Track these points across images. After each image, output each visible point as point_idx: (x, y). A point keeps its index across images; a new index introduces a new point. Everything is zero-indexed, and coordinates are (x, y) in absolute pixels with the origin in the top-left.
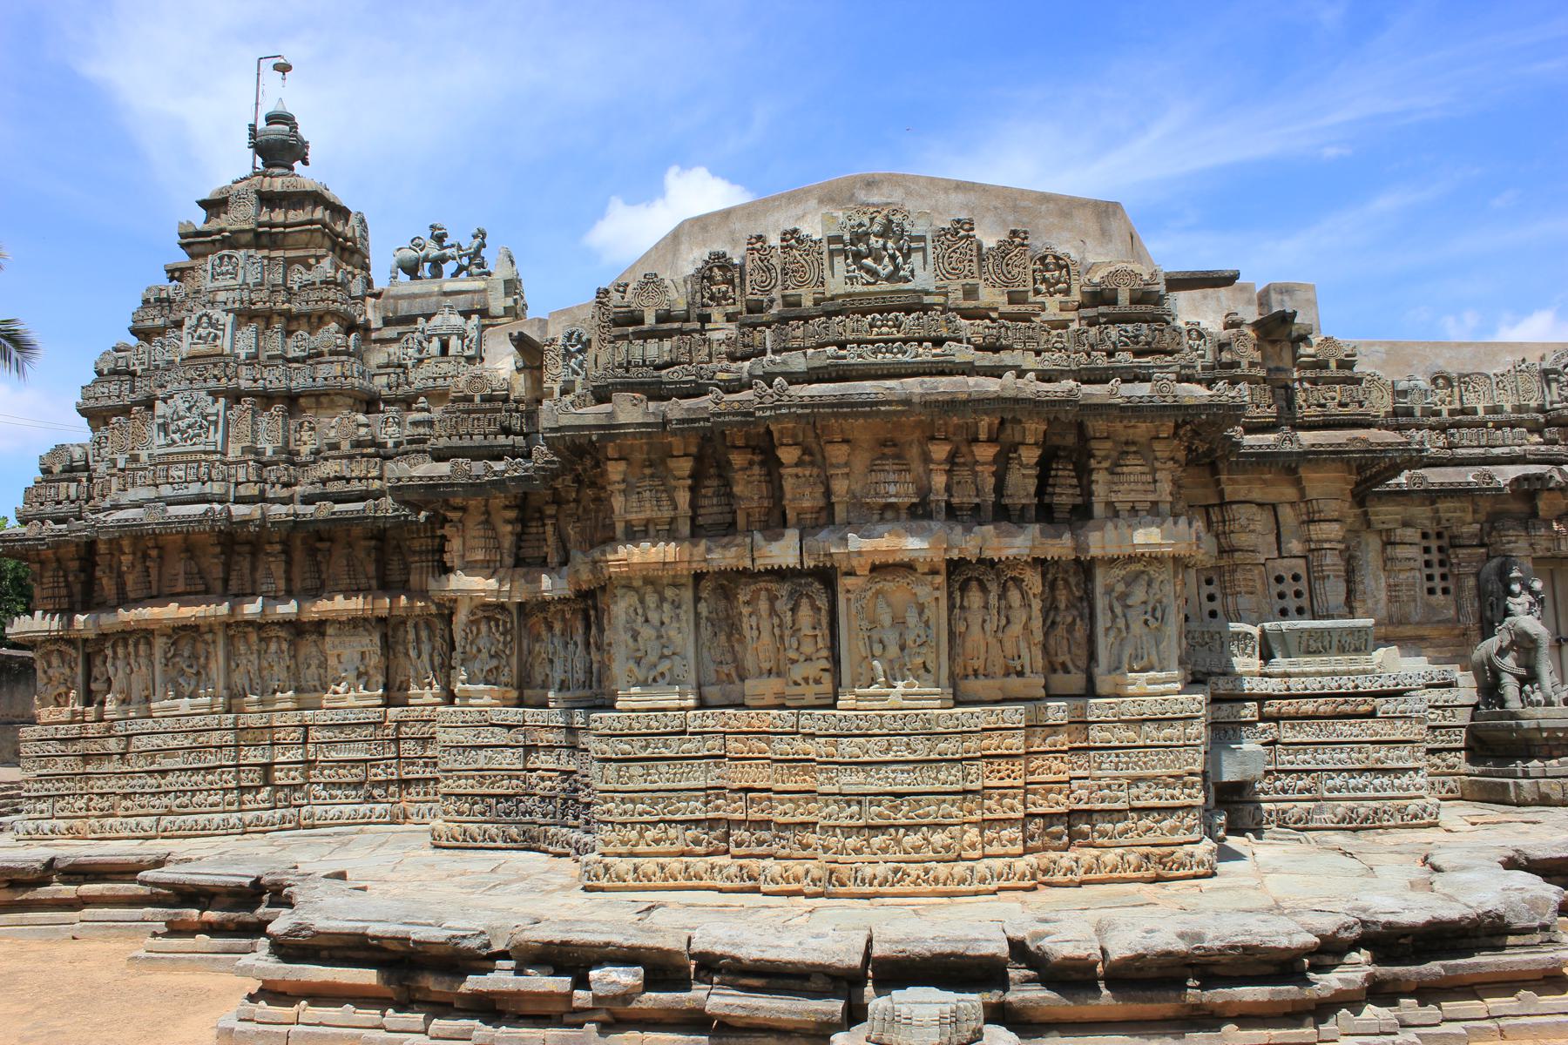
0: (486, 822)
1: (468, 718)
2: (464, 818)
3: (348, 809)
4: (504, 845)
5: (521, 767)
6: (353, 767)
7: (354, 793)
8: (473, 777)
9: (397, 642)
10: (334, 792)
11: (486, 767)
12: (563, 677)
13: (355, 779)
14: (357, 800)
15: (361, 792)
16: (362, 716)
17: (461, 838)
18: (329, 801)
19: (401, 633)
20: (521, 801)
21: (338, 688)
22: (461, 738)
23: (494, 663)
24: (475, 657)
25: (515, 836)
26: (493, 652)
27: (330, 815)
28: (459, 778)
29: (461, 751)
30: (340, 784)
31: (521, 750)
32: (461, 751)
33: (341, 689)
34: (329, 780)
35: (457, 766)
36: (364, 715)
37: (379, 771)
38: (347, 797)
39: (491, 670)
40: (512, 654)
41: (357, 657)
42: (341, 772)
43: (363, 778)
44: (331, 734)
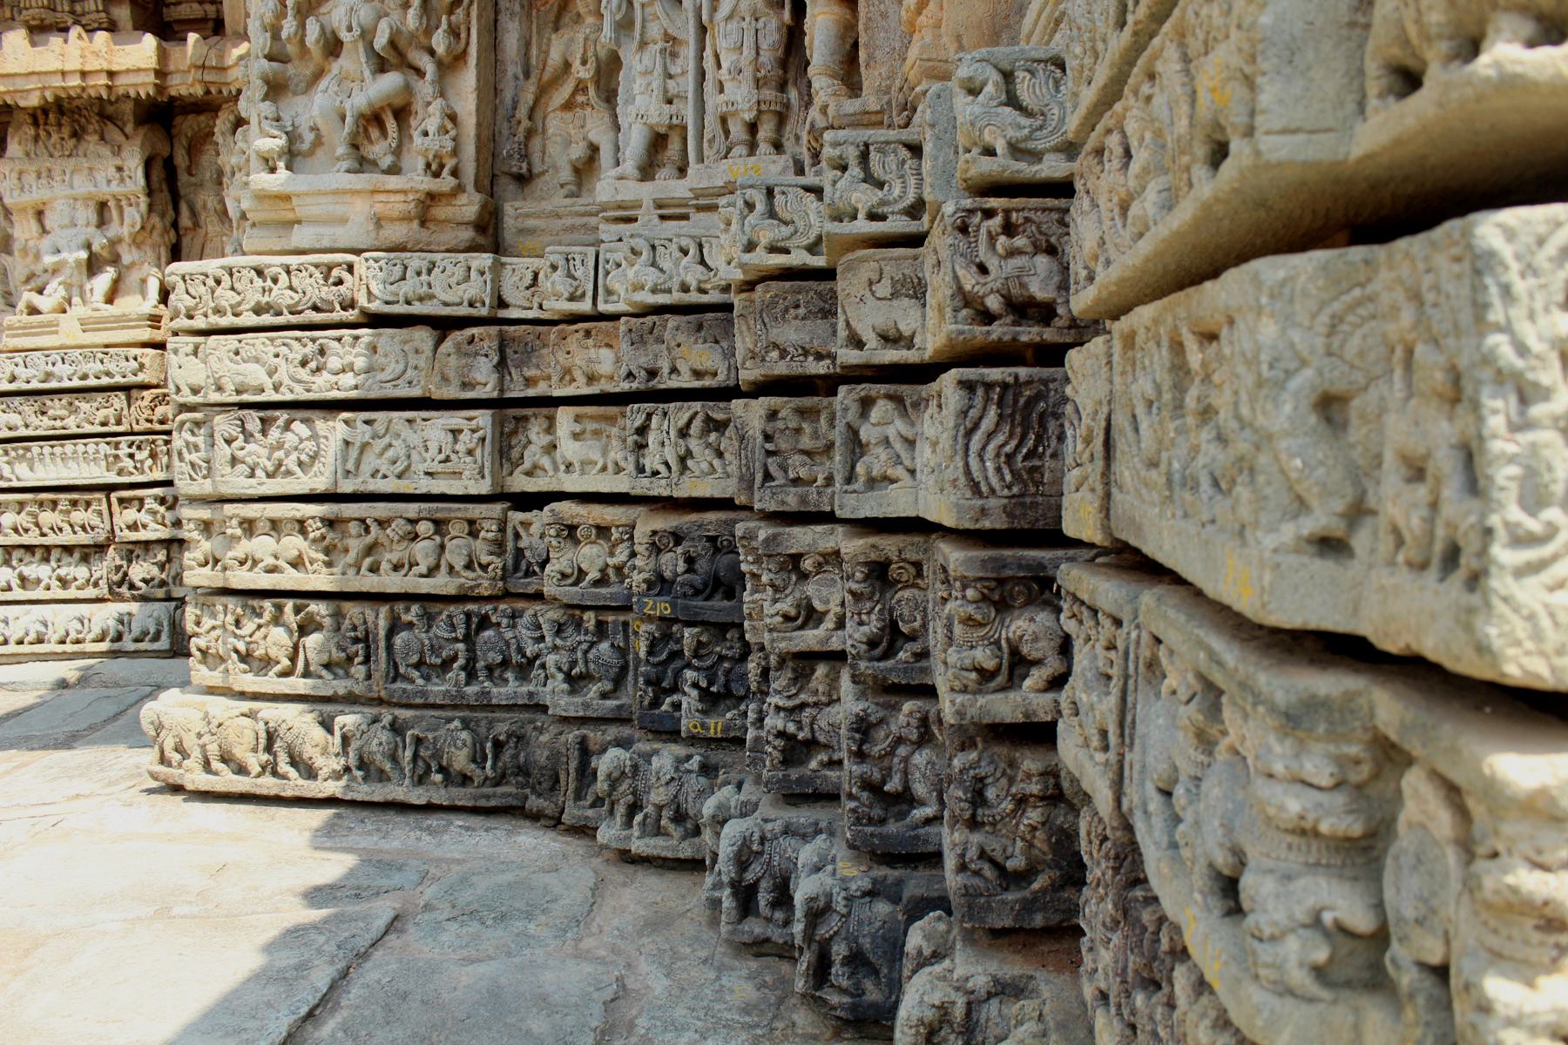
0: (351, 700)
1: (281, 295)
2: (270, 683)
3: (62, 618)
4: (417, 796)
5: (484, 488)
6: (74, 503)
7: (82, 572)
8: (301, 526)
9: (201, 185)
10: (35, 570)
11: (347, 487)
12: (658, 115)
13: (83, 538)
14: (91, 592)
15: (103, 568)
16: (92, 371)
17: (254, 762)
18: (19, 594)
19: (206, 159)
20: (484, 622)
21: (38, 301)
22: (255, 374)
23: (391, 81)
24: (319, 74)
25: (460, 760)
26: (381, 41)
27: (15, 632)
28: (249, 526)
29: (254, 424)
30: (48, 549)
31: (483, 418)
32: (253, 420)
33: (43, 302)
34: (14, 539)
35: (238, 483)
36: (98, 367)
37: (143, 517)
38: (64, 583)
39: (373, 119)
40: (457, 59)
41: (88, 214)
42: (47, 518)
43: (101, 537)
44: (15, 419)
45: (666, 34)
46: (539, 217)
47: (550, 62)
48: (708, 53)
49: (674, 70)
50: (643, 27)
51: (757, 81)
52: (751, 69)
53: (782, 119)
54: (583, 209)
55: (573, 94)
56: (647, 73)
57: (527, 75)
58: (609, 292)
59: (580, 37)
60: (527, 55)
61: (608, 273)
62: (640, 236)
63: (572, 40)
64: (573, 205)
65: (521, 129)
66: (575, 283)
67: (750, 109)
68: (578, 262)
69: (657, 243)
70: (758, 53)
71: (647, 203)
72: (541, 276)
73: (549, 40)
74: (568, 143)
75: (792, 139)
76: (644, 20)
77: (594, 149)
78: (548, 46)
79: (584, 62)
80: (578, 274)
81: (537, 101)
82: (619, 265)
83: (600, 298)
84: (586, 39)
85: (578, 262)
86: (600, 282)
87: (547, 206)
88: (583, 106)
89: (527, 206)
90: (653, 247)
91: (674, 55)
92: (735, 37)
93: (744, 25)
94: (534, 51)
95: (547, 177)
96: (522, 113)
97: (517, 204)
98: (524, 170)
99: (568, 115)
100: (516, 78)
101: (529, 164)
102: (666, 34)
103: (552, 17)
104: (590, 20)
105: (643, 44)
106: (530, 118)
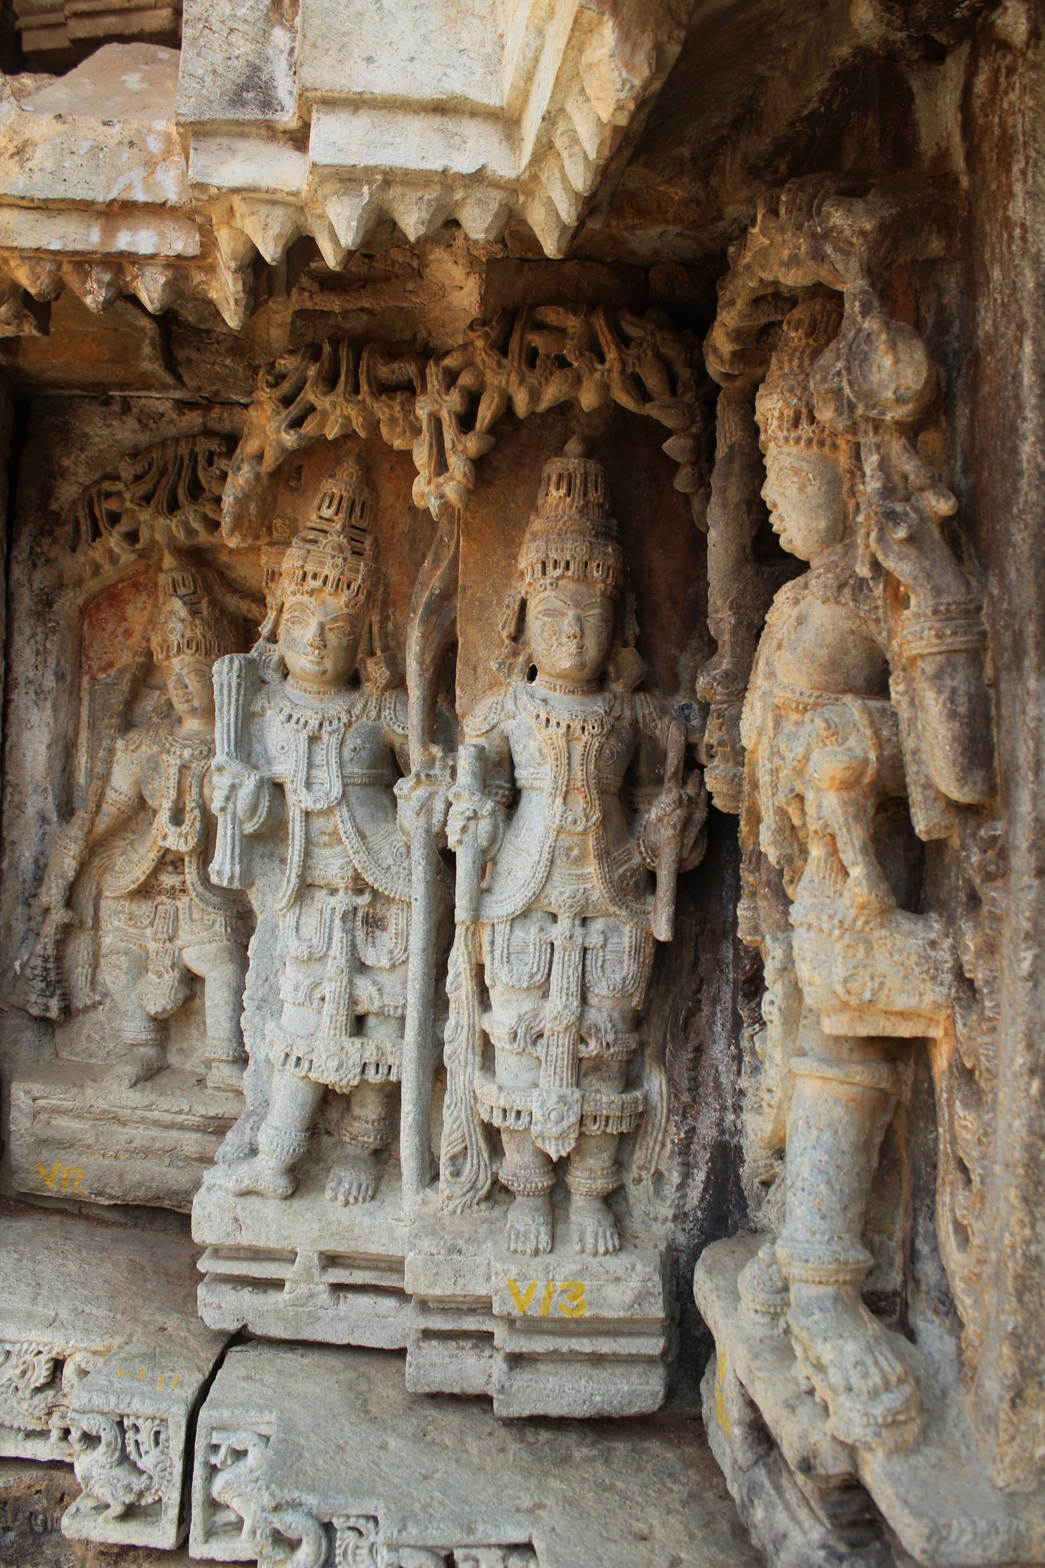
45: (357, 877)
46: (80, 1117)
47: (111, 795)
48: (458, 961)
49: (370, 956)
50: (307, 854)
51: (577, 1062)
52: (566, 1040)
53: (625, 1142)
54: (168, 1118)
55: (155, 872)
56: (312, 959)
57: (67, 811)
58: (213, 1505)
59: (171, 763)
60: (67, 771)
61: (213, 1470)
62: (294, 1505)
63: (153, 765)
64: (148, 1107)
65: (49, 930)
66: (139, 1483)
67: (562, 1137)
68: (145, 1437)
69: (337, 1522)
70: (584, 1000)
71: (307, 1254)
72: (69, 1370)
73: (111, 751)
74: (140, 967)
75: (648, 1182)
76: (308, 841)
77: (192, 982)
78: (109, 763)
79: (177, 818)
80: (145, 1463)
81: (84, 866)
82: (239, 1454)
83: (196, 1531)
84: (183, 768)
85: (145, 1437)
86: (197, 1496)
87: (94, 1097)
88: (173, 893)
89: (56, 1097)
90: (328, 1529)
91: (374, 923)
92: (530, 964)
93: (559, 932)
94: (82, 759)
95: (100, 1015)
96: (53, 893)
97: (37, 1089)
98: (54, 1013)
99: (144, 908)
100: (44, 819)
101: (66, 997)
102: (357, 877)
103: (117, 700)
104: (192, 725)
105: (305, 889)
106: (70, 902)
